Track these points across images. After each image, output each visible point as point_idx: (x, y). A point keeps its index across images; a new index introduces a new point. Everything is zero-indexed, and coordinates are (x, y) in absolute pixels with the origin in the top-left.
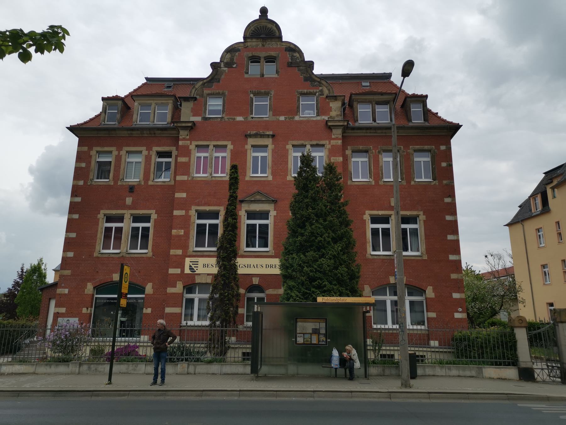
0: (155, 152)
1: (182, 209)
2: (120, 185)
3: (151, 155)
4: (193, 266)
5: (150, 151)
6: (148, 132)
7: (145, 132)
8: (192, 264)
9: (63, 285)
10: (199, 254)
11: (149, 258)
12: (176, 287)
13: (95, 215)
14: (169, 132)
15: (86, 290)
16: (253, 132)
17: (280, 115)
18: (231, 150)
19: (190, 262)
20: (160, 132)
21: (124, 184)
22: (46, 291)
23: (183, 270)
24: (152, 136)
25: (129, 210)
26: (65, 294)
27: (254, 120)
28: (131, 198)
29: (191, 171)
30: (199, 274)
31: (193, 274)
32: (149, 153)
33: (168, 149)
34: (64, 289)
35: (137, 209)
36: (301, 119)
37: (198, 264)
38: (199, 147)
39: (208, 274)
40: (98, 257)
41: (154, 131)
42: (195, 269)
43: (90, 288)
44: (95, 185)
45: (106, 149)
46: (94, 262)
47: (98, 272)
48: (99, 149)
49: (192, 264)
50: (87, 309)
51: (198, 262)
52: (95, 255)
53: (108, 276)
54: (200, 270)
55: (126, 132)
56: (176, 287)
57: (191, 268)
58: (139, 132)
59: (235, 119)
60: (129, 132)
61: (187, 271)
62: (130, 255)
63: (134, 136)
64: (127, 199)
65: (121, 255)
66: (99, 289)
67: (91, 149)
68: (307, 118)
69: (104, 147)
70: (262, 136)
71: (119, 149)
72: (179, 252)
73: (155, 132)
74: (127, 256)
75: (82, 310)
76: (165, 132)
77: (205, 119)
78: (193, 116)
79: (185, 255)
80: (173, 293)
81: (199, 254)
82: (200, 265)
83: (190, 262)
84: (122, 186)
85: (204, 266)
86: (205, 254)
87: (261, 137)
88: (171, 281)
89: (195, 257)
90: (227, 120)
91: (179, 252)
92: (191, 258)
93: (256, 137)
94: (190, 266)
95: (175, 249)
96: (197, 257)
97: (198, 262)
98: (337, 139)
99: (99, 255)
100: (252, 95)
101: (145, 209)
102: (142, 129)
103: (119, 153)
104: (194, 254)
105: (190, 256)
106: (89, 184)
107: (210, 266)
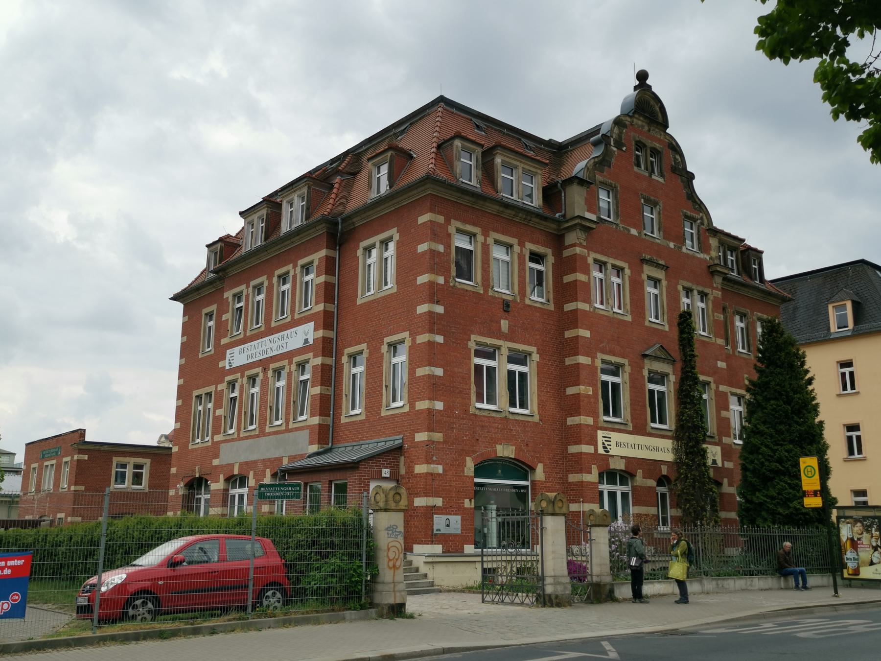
0: (529, 251)
1: (588, 356)
2: (491, 296)
3: (525, 255)
4: (606, 443)
5: (523, 248)
6: (524, 216)
7: (520, 215)
8: (606, 441)
9: (434, 458)
10: (610, 426)
11: (536, 424)
12: (591, 473)
13: (465, 342)
14: (548, 224)
15: (465, 468)
16: (648, 257)
17: (670, 240)
18: (629, 277)
19: (603, 437)
20: (537, 220)
21: (497, 296)
22: (363, 465)
23: (596, 449)
24: (525, 223)
25: (507, 341)
26: (439, 475)
27: (647, 238)
28: (507, 322)
29: (592, 298)
30: (613, 456)
31: (607, 457)
32: (522, 250)
33: (544, 251)
34: (436, 466)
35: (514, 342)
36: (688, 252)
37: (610, 441)
38: (602, 265)
39: (622, 457)
40: (474, 415)
41: (531, 217)
42: (608, 447)
43: (470, 465)
44: (459, 289)
45: (469, 228)
46: (471, 423)
47: (477, 440)
48: (460, 225)
49: (606, 441)
50: (470, 500)
51: (610, 438)
52: (472, 410)
53: (490, 448)
54: (614, 451)
55: (497, 207)
56: (591, 473)
57: (604, 448)
58: (514, 213)
59: (629, 231)
60: (501, 209)
61: (601, 451)
62: (515, 415)
63: (483, 209)
64: (502, 322)
65: (503, 415)
66: (480, 470)
67: (448, 221)
68: (693, 252)
69: (466, 223)
70: (658, 266)
71: (486, 234)
72: (590, 421)
73: (532, 219)
74: (511, 417)
75: (464, 503)
76: (544, 223)
77: (599, 218)
78: (588, 211)
79: (596, 427)
80: (588, 482)
81: (610, 426)
82: (613, 443)
83: (603, 437)
84: (493, 297)
85: (618, 444)
86: (617, 426)
87: (655, 267)
88: (579, 463)
89: (606, 430)
90: (622, 229)
91: (590, 421)
92: (603, 432)
93: (651, 265)
94: (603, 444)
95: (586, 416)
96: (609, 431)
97: (610, 438)
98: (716, 289)
99: (477, 412)
100: (642, 201)
101: (524, 343)
102: (507, 206)
103: (485, 240)
104: (605, 425)
105: (602, 429)
106: (452, 284)
107: (622, 445)
